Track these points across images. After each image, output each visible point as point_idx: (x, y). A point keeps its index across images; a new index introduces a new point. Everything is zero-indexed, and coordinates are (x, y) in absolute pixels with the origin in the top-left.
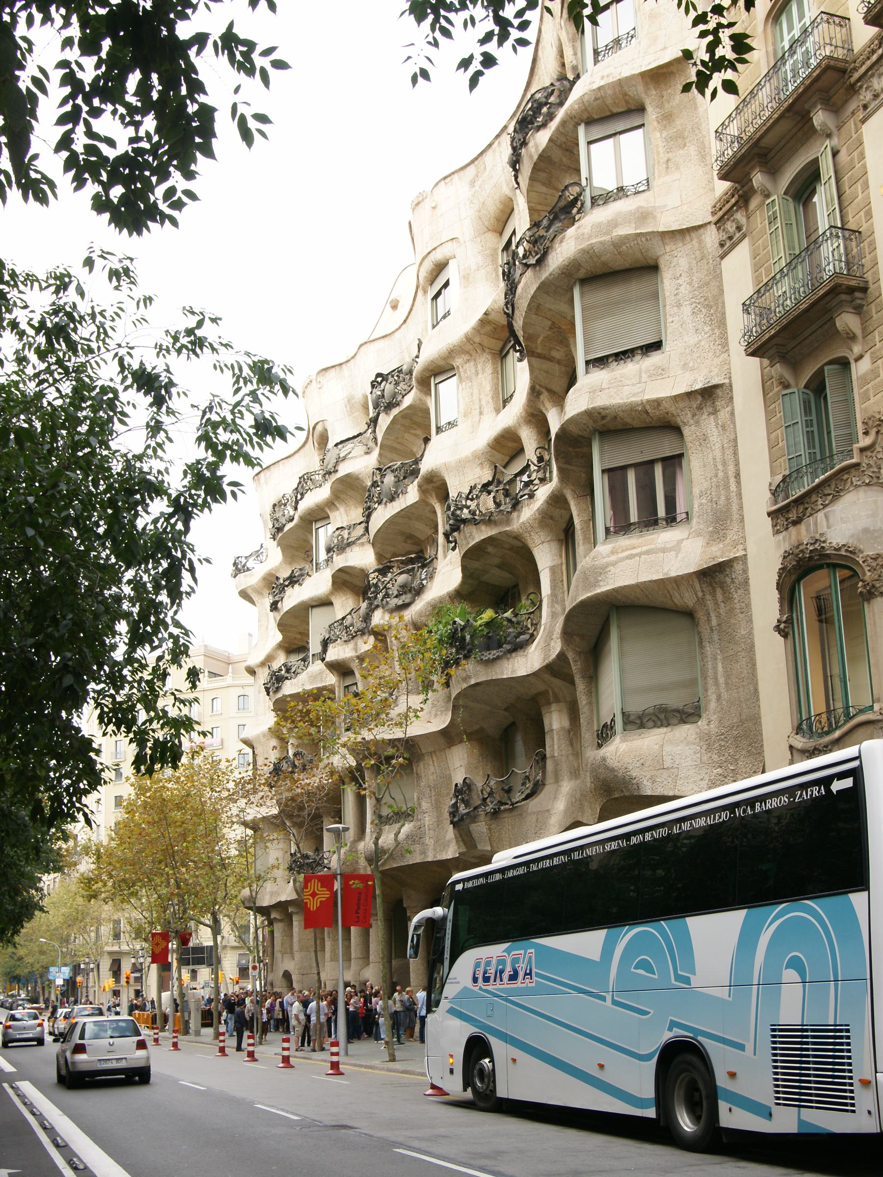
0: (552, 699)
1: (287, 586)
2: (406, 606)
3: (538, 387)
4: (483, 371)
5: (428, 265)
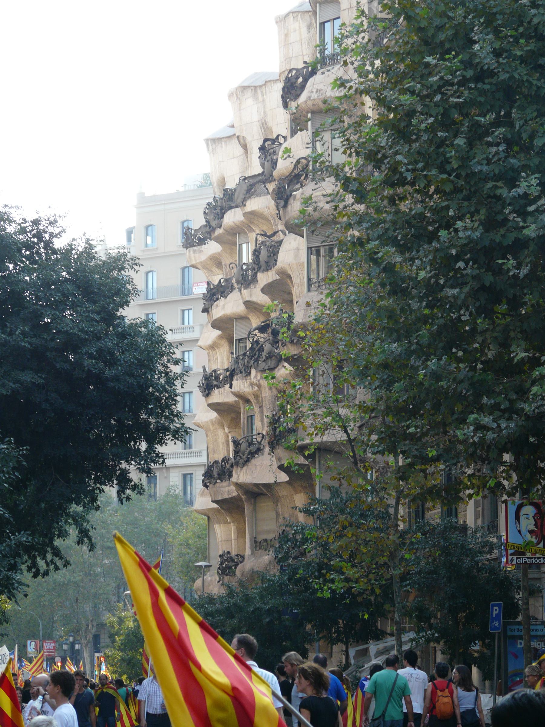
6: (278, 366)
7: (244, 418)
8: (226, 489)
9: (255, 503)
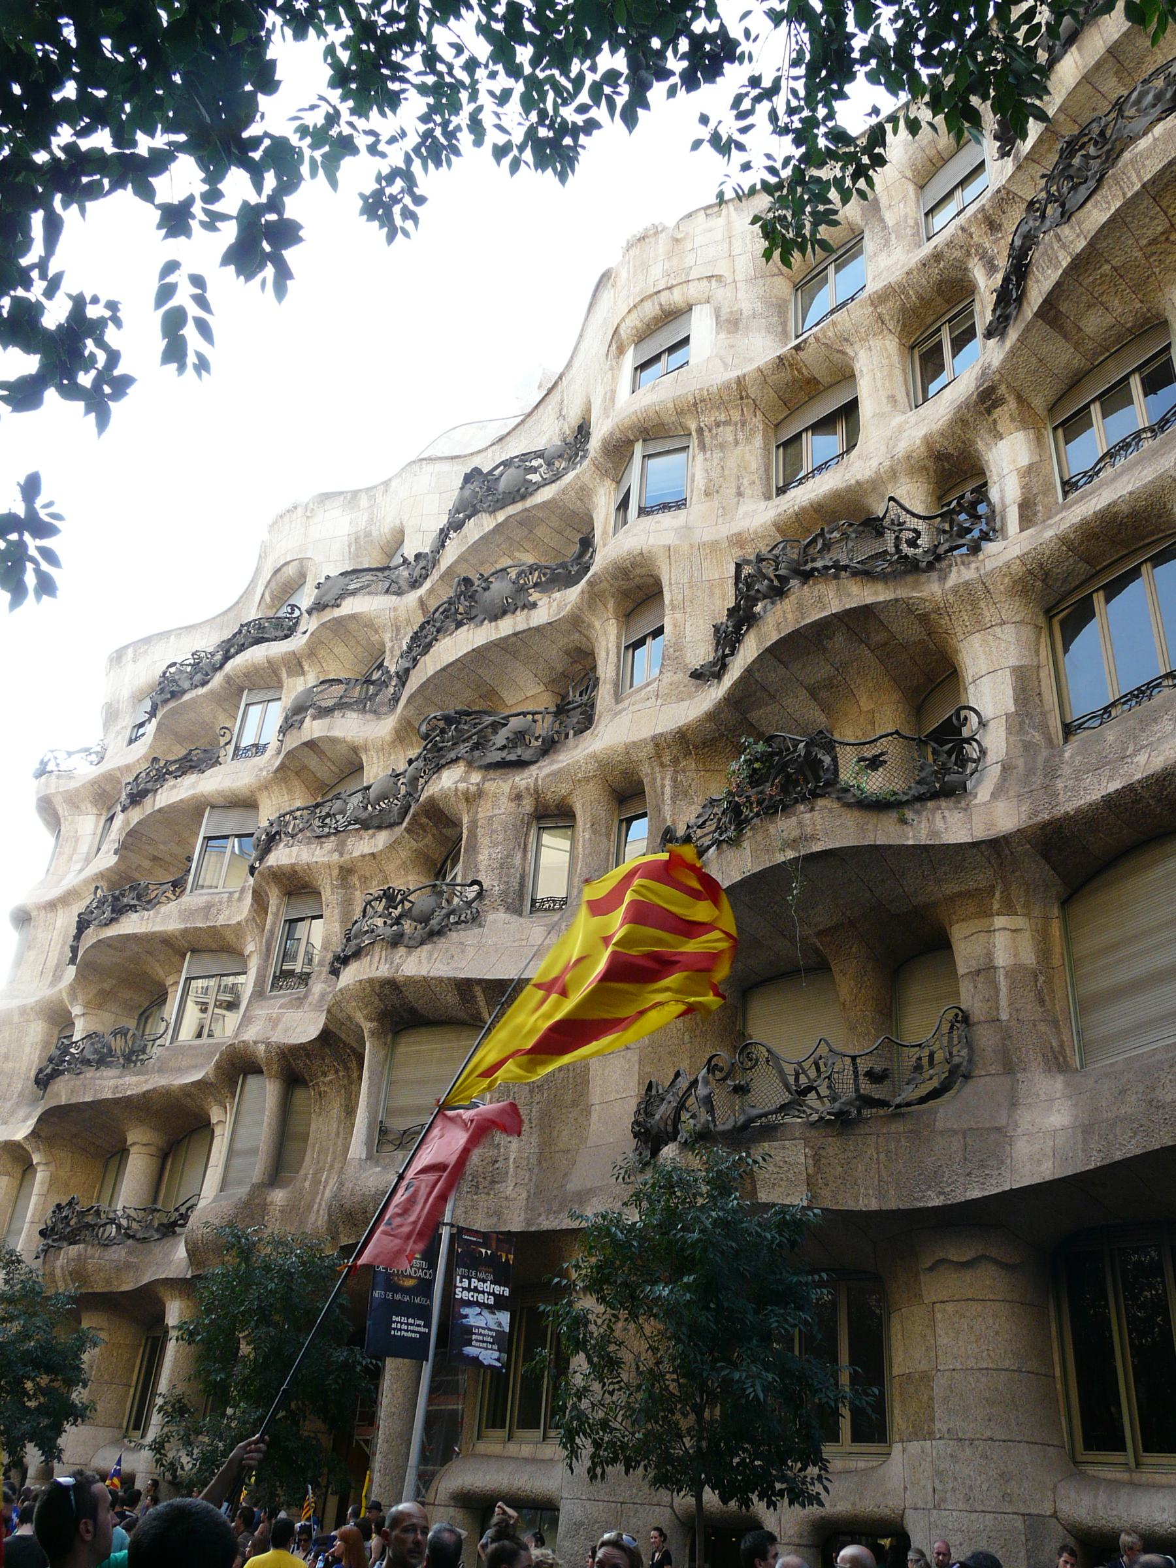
0: (996, 907)
1: (170, 773)
2: (521, 764)
3: (1002, 390)
4: (748, 440)
5: (650, 310)
6: (536, 762)
7: (274, 924)
8: (112, 1082)
9: (394, 1045)
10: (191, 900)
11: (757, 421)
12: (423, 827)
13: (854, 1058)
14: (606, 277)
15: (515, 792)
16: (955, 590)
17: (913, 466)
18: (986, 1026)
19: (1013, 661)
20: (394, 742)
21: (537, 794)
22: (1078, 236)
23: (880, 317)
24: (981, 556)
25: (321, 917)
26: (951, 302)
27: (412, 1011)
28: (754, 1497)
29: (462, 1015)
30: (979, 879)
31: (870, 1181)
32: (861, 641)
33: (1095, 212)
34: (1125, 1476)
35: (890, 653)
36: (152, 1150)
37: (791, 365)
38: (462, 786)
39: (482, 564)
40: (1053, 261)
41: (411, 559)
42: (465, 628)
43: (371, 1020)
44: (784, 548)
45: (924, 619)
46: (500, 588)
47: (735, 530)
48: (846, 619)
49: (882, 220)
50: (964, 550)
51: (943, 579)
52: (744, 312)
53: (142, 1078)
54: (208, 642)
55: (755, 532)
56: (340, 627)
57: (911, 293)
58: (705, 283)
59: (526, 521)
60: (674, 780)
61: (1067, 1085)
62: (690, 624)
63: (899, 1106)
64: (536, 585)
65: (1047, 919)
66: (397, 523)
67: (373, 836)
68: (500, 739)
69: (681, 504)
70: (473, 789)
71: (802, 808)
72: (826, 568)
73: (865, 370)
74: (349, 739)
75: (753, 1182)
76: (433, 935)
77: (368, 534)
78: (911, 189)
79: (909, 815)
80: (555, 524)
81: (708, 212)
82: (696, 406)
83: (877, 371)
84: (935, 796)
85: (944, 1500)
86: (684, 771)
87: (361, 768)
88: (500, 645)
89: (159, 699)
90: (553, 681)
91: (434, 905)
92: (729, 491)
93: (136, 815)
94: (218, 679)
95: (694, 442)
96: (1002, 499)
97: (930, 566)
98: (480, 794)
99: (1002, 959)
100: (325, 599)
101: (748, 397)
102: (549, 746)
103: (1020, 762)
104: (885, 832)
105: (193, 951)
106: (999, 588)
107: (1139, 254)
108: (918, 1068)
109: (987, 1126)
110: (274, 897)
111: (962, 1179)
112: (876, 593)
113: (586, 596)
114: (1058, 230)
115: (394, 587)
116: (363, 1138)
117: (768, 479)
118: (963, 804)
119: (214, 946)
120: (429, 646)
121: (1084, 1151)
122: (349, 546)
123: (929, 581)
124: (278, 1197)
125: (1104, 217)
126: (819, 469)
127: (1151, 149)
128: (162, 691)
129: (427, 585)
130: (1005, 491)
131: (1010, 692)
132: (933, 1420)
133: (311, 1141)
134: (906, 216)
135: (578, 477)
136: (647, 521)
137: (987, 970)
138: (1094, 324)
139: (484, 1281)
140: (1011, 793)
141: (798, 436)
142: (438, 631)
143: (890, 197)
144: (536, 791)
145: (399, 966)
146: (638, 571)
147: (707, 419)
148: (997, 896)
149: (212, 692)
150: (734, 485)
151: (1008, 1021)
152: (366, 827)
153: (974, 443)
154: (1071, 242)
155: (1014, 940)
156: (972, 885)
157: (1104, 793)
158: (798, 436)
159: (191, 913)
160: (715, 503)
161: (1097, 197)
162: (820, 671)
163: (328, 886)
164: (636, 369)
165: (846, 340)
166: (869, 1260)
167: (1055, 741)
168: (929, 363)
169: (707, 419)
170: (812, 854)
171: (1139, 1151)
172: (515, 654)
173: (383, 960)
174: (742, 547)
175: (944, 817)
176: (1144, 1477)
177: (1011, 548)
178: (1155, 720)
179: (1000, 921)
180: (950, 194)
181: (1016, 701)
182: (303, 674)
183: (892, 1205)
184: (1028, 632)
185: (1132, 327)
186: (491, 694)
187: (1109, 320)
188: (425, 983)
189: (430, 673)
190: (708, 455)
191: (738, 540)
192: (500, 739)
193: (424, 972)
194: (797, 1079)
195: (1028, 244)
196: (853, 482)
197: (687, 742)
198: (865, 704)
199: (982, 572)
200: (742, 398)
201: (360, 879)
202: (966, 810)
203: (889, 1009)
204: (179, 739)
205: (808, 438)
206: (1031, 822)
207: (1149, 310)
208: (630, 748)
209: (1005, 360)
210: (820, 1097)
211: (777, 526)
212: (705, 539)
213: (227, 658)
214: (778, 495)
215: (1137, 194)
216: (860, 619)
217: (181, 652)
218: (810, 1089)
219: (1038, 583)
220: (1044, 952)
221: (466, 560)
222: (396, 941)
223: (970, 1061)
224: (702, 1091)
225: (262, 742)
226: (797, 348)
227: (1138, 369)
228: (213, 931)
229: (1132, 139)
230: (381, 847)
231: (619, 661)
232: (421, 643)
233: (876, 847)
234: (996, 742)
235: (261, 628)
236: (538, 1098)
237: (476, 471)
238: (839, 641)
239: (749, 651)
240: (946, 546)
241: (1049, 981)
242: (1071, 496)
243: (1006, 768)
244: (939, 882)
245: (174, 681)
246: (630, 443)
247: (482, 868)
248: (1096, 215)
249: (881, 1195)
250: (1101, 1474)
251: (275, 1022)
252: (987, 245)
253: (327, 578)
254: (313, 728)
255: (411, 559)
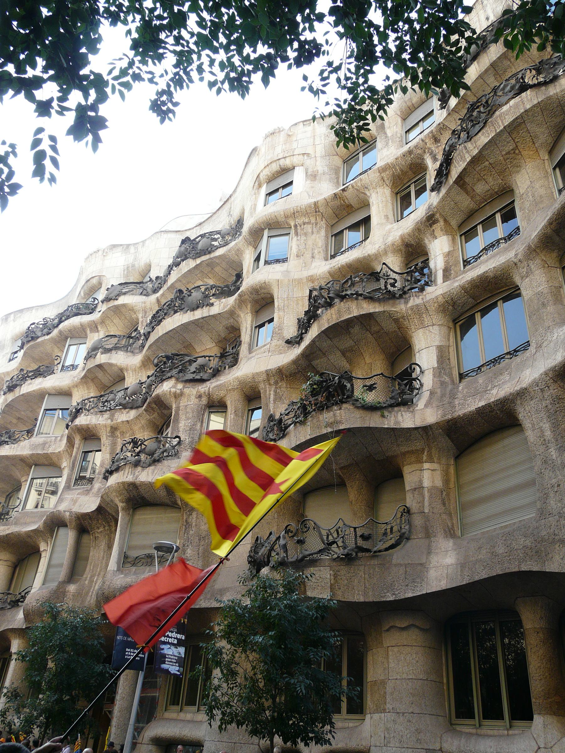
0: (425, 458)
1: (29, 377)
2: (202, 381)
5: (275, 167)
7: (77, 453)
10: (36, 440)
11: (323, 223)
12: (153, 409)
13: (355, 528)
14: (254, 150)
15: (199, 394)
16: (412, 308)
17: (395, 249)
18: (418, 515)
19: (437, 343)
20: (141, 367)
21: (209, 396)
22: (474, 148)
23: (382, 178)
24: (424, 293)
25: (100, 451)
26: (416, 173)
27: (143, 498)
28: (299, 740)
29: (167, 501)
30: (418, 445)
31: (361, 587)
32: (367, 330)
33: (482, 137)
34: (474, 731)
35: (380, 336)
36: (9, 563)
37: (340, 198)
38: (173, 390)
39: (188, 283)
40: (463, 158)
41: (154, 279)
42: (178, 313)
43: (123, 502)
44: (332, 284)
45: (396, 321)
46: (196, 295)
47: (310, 274)
48: (360, 319)
49: (385, 133)
50: (417, 290)
51: (406, 303)
52: (319, 172)
53: (6, 527)
54: (51, 314)
55: (320, 275)
56: (117, 310)
57: (397, 168)
58: (301, 156)
59: (211, 264)
60: (275, 392)
61: (455, 544)
62: (287, 317)
63: (375, 552)
64: (213, 295)
65: (448, 465)
66: (148, 261)
67: (128, 412)
68: (193, 368)
69: (285, 260)
70: (178, 391)
71: (335, 408)
72: (352, 294)
73: (374, 202)
74: (118, 364)
75: (305, 586)
76: (155, 462)
77: (133, 266)
78: (399, 120)
79: (386, 413)
80: (224, 267)
81: (305, 123)
82: (294, 214)
83: (380, 203)
84: (398, 405)
85: (389, 742)
86: (280, 388)
87: (124, 379)
88: (195, 323)
89: (25, 341)
90: (220, 341)
91: (156, 447)
92: (308, 255)
93: (10, 397)
94: (55, 332)
95: (293, 231)
96: (435, 266)
97: (401, 296)
98: (182, 394)
99: (426, 483)
100: (110, 296)
101: (319, 211)
102: (216, 373)
103: (439, 391)
104: (374, 421)
105: (36, 465)
106: (433, 308)
107: (502, 158)
108: (385, 534)
109: (417, 562)
110: (77, 440)
111: (404, 588)
112: (375, 308)
113: (238, 301)
114: (466, 144)
115: (145, 292)
116: (116, 560)
117: (327, 250)
118: (411, 409)
119: (46, 463)
120: (161, 321)
121: (461, 575)
122: (124, 271)
123: (400, 304)
124: (72, 588)
125: (487, 140)
126: (351, 248)
127: (508, 111)
128: (27, 336)
129: (161, 292)
130: (437, 262)
131: (435, 358)
132: (385, 703)
133: (90, 561)
134: (397, 132)
135: (236, 244)
136: (268, 267)
137: (419, 488)
138: (480, 188)
139: (172, 632)
140: (434, 405)
141: (342, 231)
142: (165, 315)
143: (390, 123)
144: (209, 394)
145: (137, 476)
146: (263, 291)
147: (299, 221)
148: (425, 453)
149: (52, 338)
150: (310, 253)
151: (428, 513)
152: (125, 408)
153: (423, 240)
154: (472, 150)
155: (432, 475)
156: (414, 448)
157: (477, 407)
158: (342, 231)
159: (36, 446)
160: (301, 261)
161: (483, 131)
162: (347, 343)
163: (105, 436)
164: (267, 195)
165: (366, 188)
166: (359, 625)
167: (455, 381)
168: (404, 201)
169: (299, 221)
170: (339, 430)
171: (486, 576)
172: (202, 328)
173: (130, 473)
174: (313, 282)
175: (402, 415)
176: (483, 731)
177: (438, 290)
178: (501, 374)
179: (426, 466)
180: (417, 123)
181: (438, 362)
182: (98, 331)
183: (371, 599)
184: (445, 330)
185: (498, 191)
186: (189, 346)
187: (487, 187)
188: (150, 485)
189: (160, 334)
190: (299, 238)
191: (311, 279)
192: (193, 368)
193: (150, 480)
194: (328, 538)
195: (452, 149)
196: (366, 255)
197: (282, 374)
198: (368, 360)
199: (425, 300)
200: (316, 212)
201: (120, 433)
202: (412, 412)
203: (372, 506)
204: (34, 360)
205: (346, 233)
206: (443, 419)
207: (505, 184)
208: (254, 376)
209: (439, 203)
210: (338, 547)
211: (331, 273)
212: (296, 277)
213: (60, 322)
214: (331, 259)
215: (501, 131)
216: (366, 319)
217: (37, 317)
218: (334, 542)
219: (450, 307)
220: (446, 481)
221: (180, 281)
222: (136, 464)
223: (410, 531)
224: (282, 542)
225: (76, 364)
226: (343, 190)
227: (500, 211)
228: (46, 456)
229: (500, 106)
230: (132, 418)
231: (252, 333)
232: (157, 319)
233: (369, 429)
234: (428, 381)
235: (78, 308)
236: (202, 543)
237: (188, 239)
238: (356, 330)
239: (314, 332)
240: (409, 287)
241: (448, 495)
242: (467, 267)
243: (432, 393)
244: (398, 445)
245: (33, 332)
246: (262, 230)
247: (181, 430)
248: (483, 139)
249: (365, 594)
250: (463, 730)
251: (75, 502)
252: (433, 149)
253: (112, 286)
254: (101, 358)
255: (154, 279)
